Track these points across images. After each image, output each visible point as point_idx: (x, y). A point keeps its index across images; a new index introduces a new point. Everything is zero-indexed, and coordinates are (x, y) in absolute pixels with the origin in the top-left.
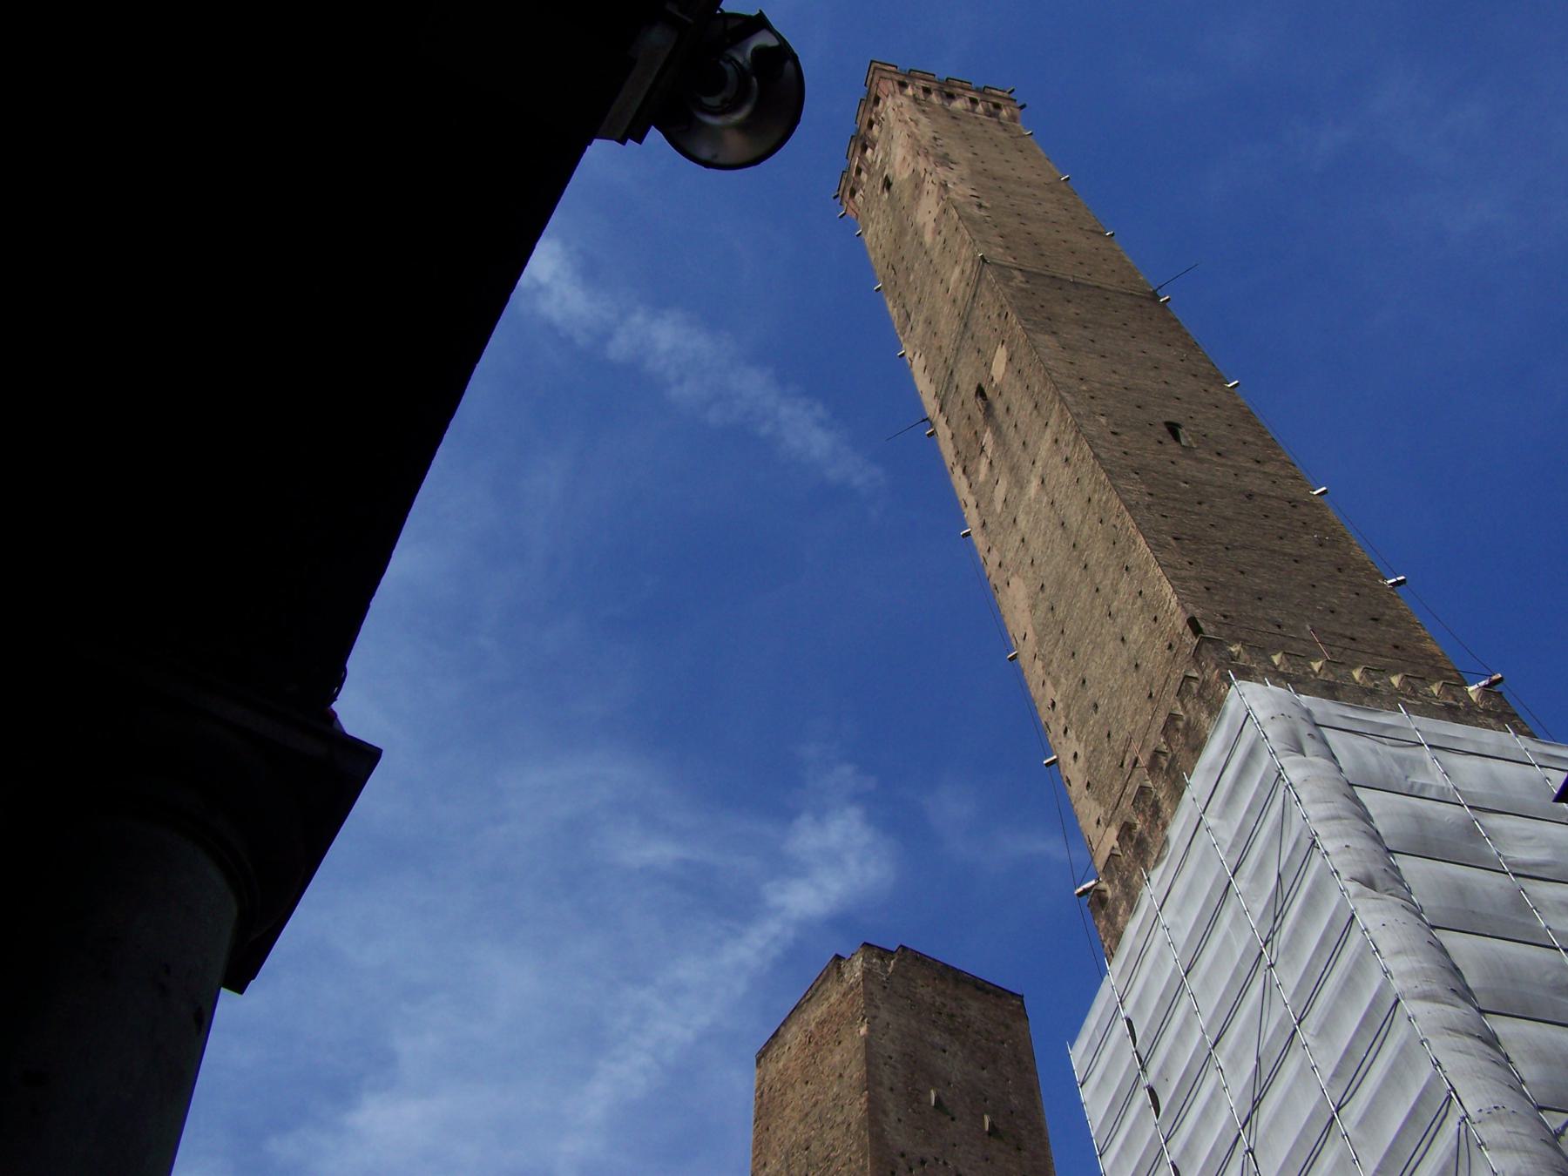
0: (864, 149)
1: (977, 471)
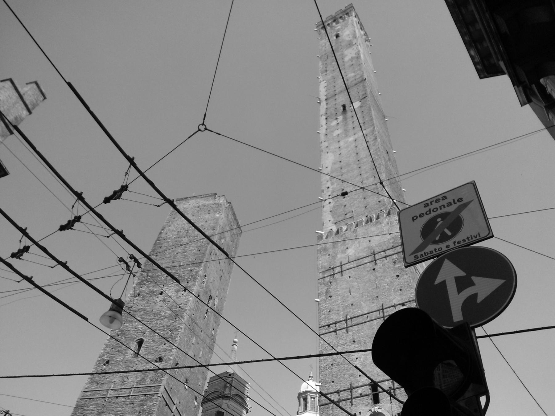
0: (334, 21)
1: (331, 122)
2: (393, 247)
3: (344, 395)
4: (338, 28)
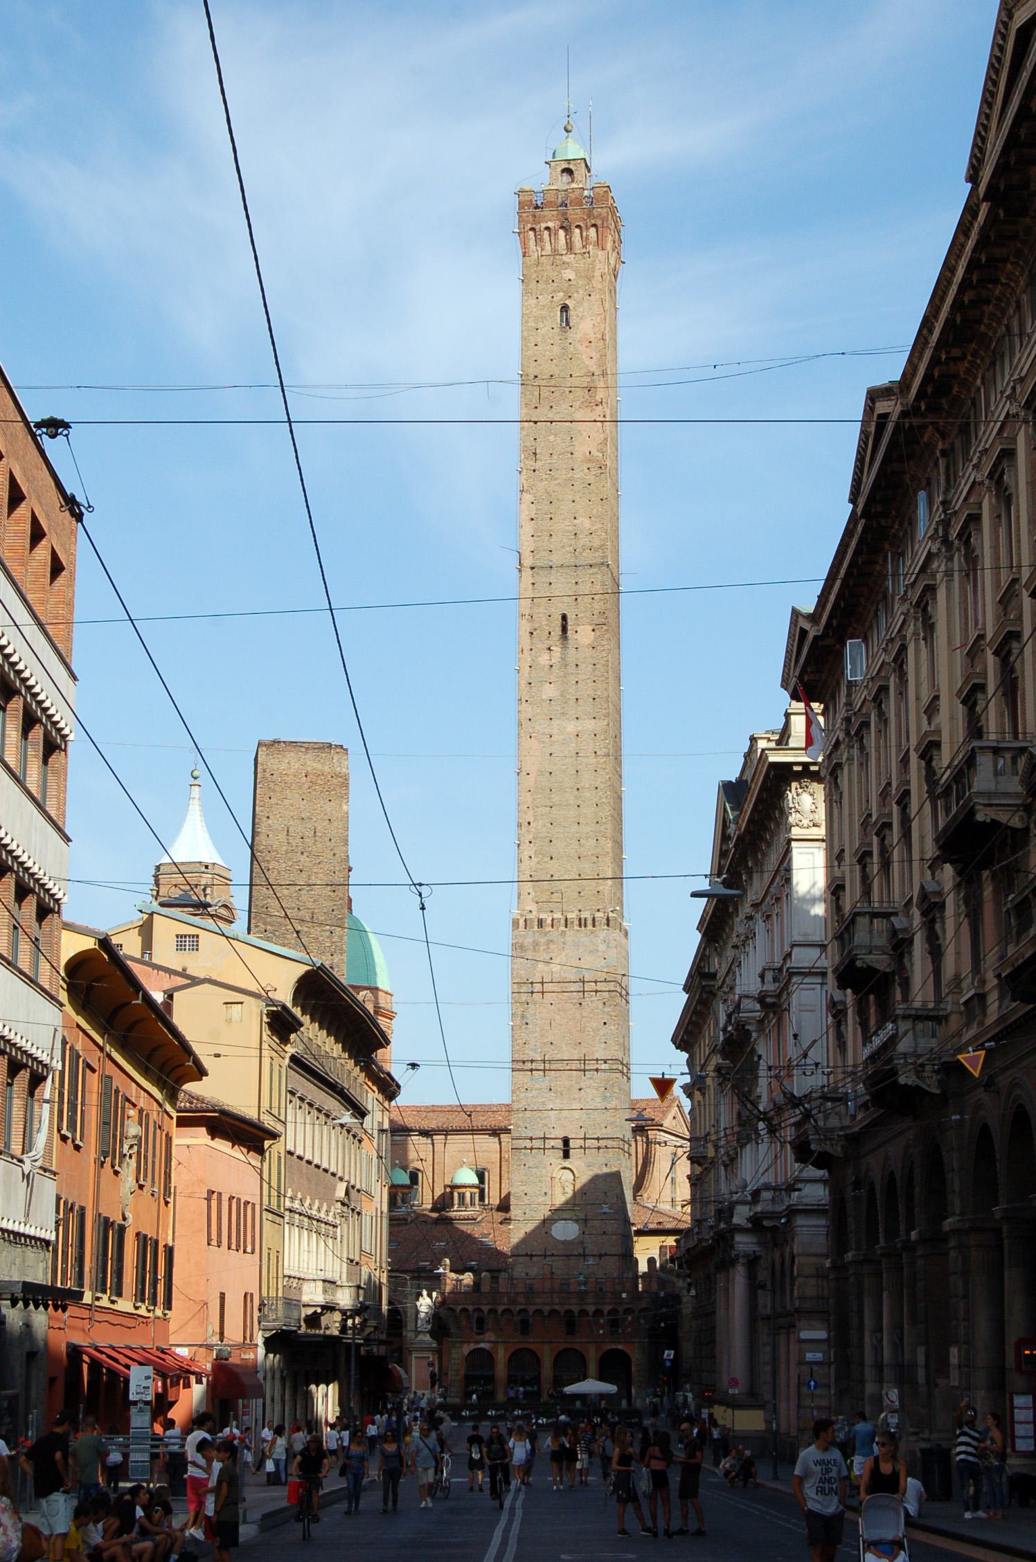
2: (605, 981)
3: (537, 1144)
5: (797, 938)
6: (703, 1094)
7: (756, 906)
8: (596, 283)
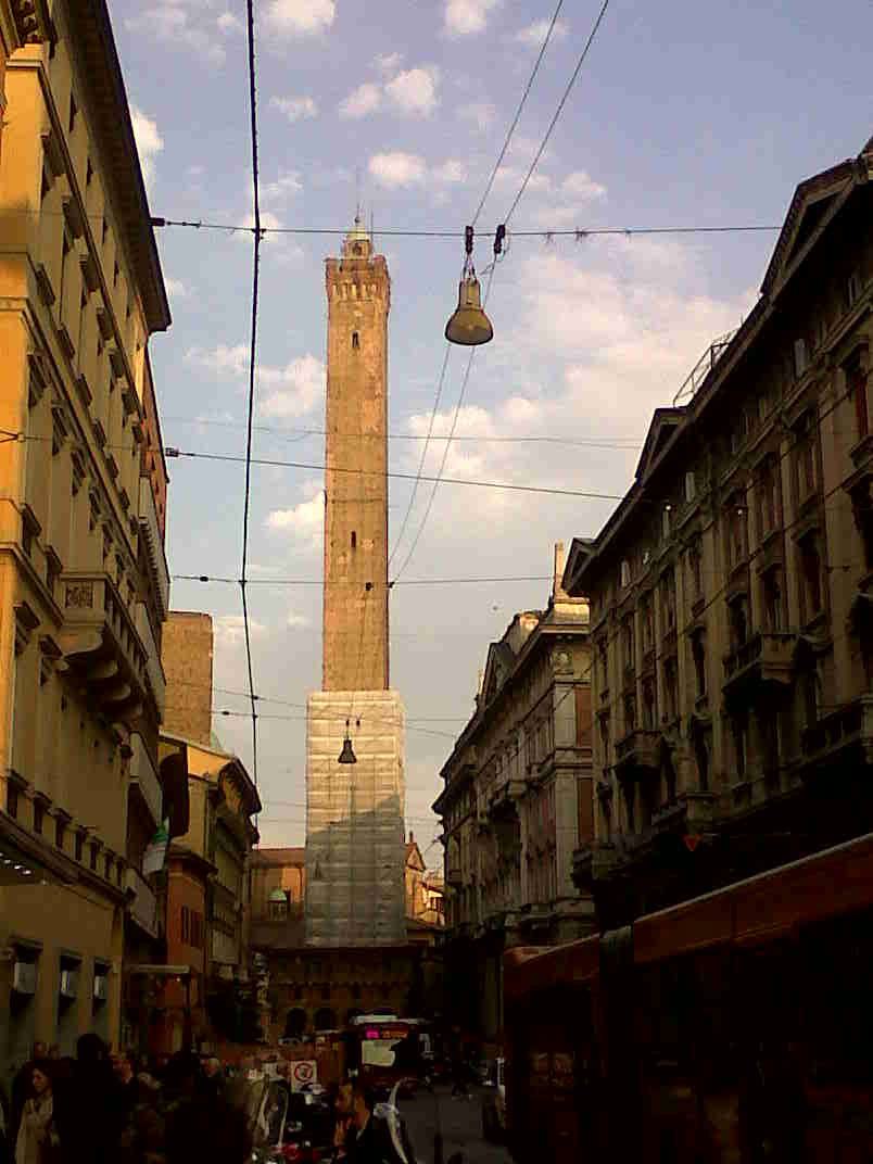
4: (357, 314)
5: (558, 745)
6: (459, 842)
7: (520, 723)
8: (376, 320)
